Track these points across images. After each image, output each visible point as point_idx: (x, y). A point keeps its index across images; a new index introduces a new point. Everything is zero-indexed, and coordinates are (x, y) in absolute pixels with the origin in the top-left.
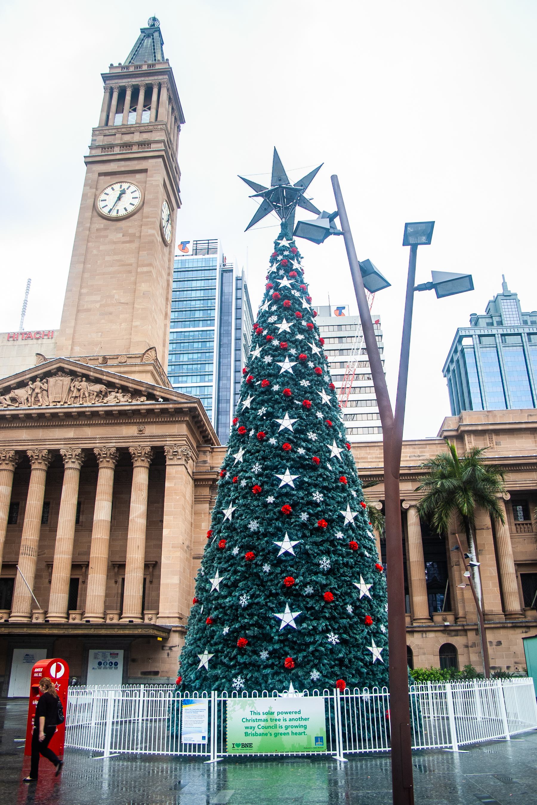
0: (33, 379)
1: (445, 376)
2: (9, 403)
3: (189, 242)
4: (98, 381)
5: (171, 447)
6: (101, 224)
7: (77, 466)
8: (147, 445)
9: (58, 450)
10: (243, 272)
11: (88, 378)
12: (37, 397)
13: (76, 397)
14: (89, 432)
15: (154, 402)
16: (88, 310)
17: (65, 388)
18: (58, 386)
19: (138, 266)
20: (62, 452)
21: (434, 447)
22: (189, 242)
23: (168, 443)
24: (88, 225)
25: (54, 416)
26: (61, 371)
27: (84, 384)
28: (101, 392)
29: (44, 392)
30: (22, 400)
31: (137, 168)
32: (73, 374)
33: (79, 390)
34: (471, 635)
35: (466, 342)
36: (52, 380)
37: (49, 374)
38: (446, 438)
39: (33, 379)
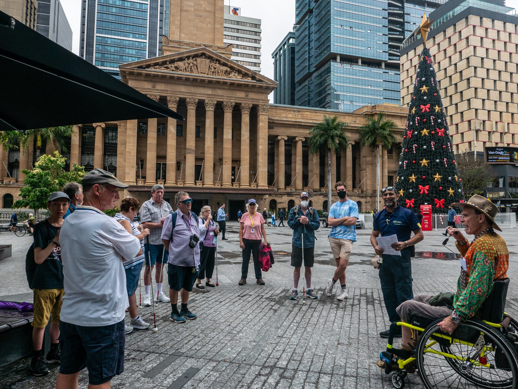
0: (188, 58)
1: (273, 58)
2: (174, 69)
4: (225, 65)
5: (263, 105)
7: (213, 110)
8: (250, 104)
9: (204, 100)
12: (191, 68)
13: (213, 72)
14: (220, 92)
16: (187, 11)
17: (207, 65)
18: (203, 63)
20: (206, 101)
21: (360, 118)
23: (261, 103)
25: (203, 81)
26: (203, 54)
27: (217, 65)
28: (227, 71)
29: (195, 66)
30: (182, 69)
32: (210, 58)
33: (215, 68)
34: (368, 199)
35: (291, 41)
36: (199, 60)
37: (196, 56)
38: (366, 115)
39: (188, 58)
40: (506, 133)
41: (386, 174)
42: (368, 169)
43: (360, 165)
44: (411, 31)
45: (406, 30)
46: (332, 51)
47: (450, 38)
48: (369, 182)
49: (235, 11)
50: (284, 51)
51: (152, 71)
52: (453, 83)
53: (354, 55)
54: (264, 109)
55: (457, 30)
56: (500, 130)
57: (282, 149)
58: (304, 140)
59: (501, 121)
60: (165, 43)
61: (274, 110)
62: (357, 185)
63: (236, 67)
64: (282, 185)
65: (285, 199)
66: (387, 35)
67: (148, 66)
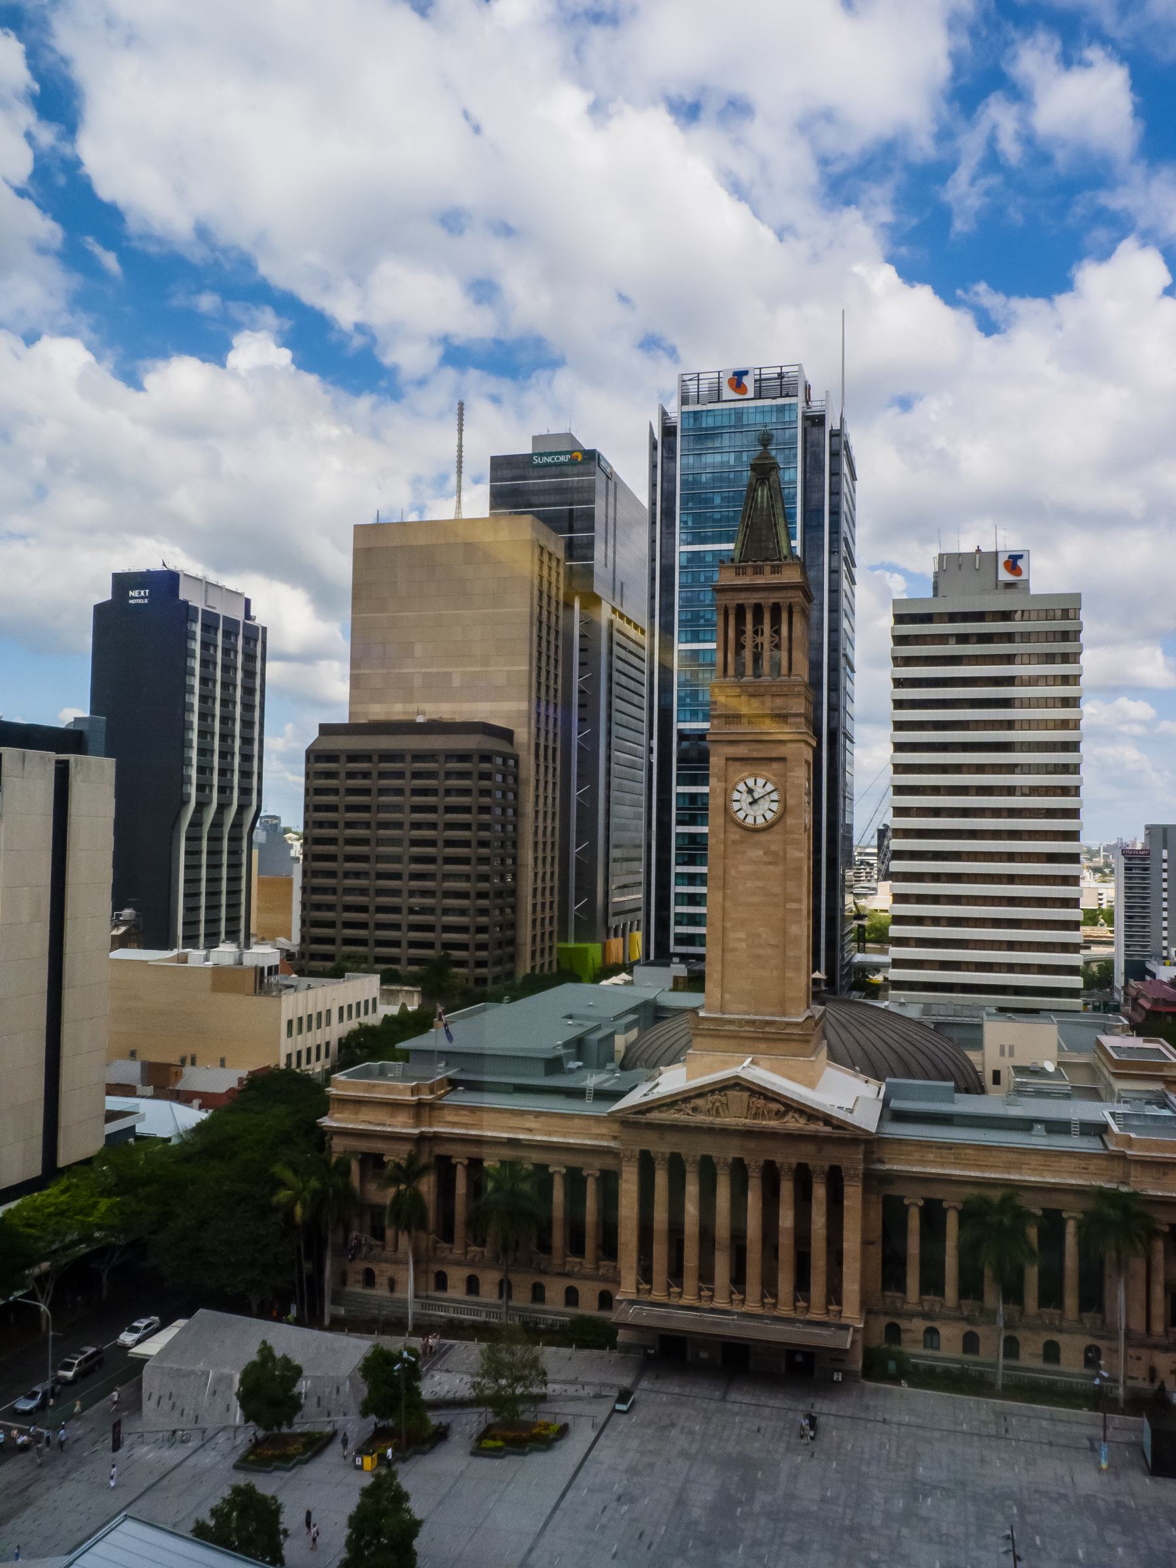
0: (712, 1092)
3: (746, 373)
6: (735, 835)
7: (759, 1175)
10: (842, 419)
11: (766, 1098)
15: (829, 1129)
16: (734, 950)
19: (786, 901)
21: (1100, 1162)
22: (746, 373)
23: (845, 1164)
24: (722, 836)
26: (736, 1084)
31: (774, 755)
36: (730, 1093)
39: (712, 1092)
49: (1014, 562)
51: (655, 1116)
54: (852, 1178)
57: (914, 1222)
58: (960, 1206)
61: (895, 1146)
63: (795, 1105)
65: (918, 1326)
67: (650, 1110)
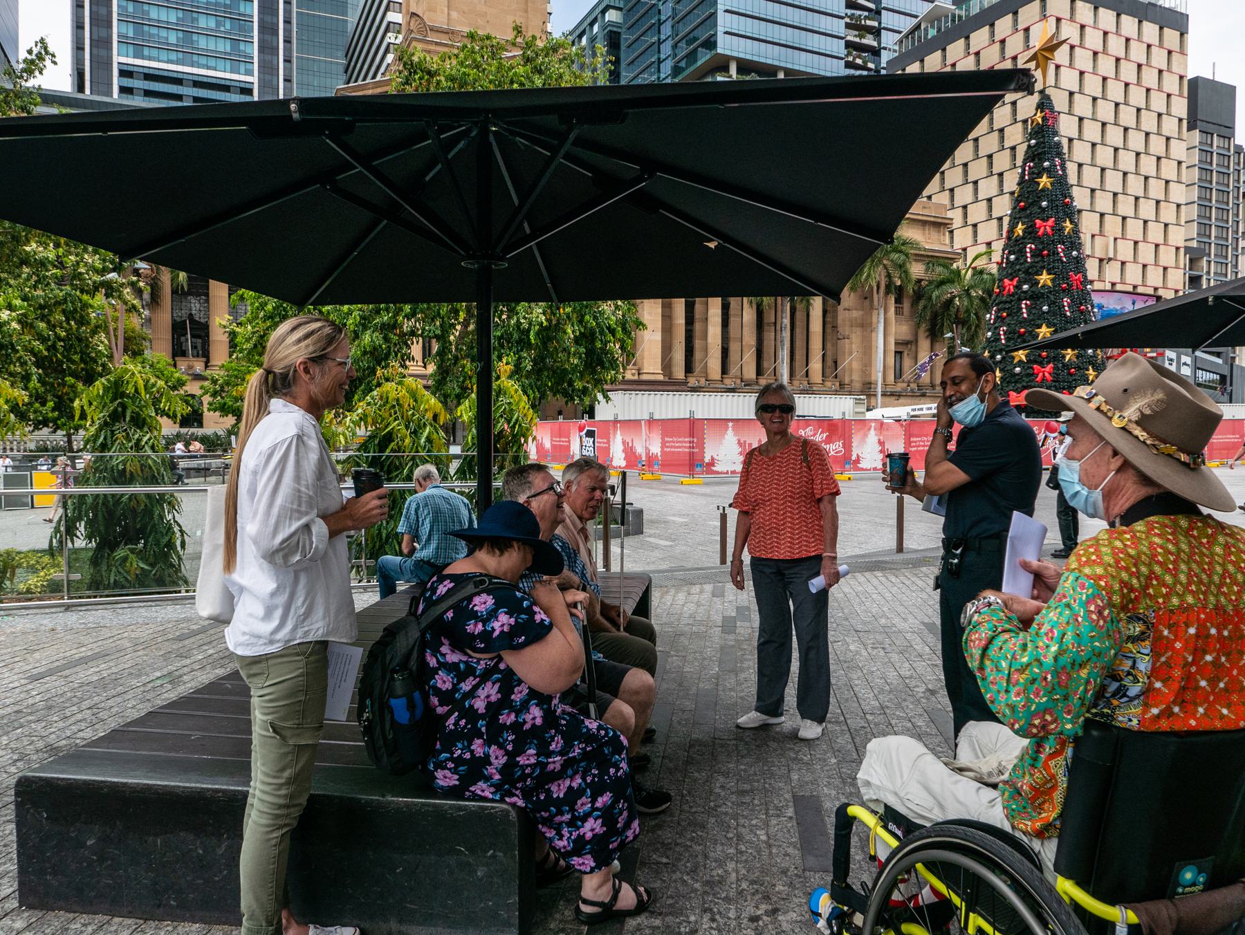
40: (1110, 259)
41: (892, 347)
42: (853, 336)
43: (835, 327)
44: (916, 17)
45: (885, 9)
46: (719, 51)
47: (1003, 42)
48: (855, 365)
50: (592, 40)
52: (1007, 144)
53: (769, 62)
55: (1021, 26)
56: (1099, 254)
59: (1101, 234)
60: (419, 32)
62: (828, 371)
64: (679, 373)
66: (842, 18)
